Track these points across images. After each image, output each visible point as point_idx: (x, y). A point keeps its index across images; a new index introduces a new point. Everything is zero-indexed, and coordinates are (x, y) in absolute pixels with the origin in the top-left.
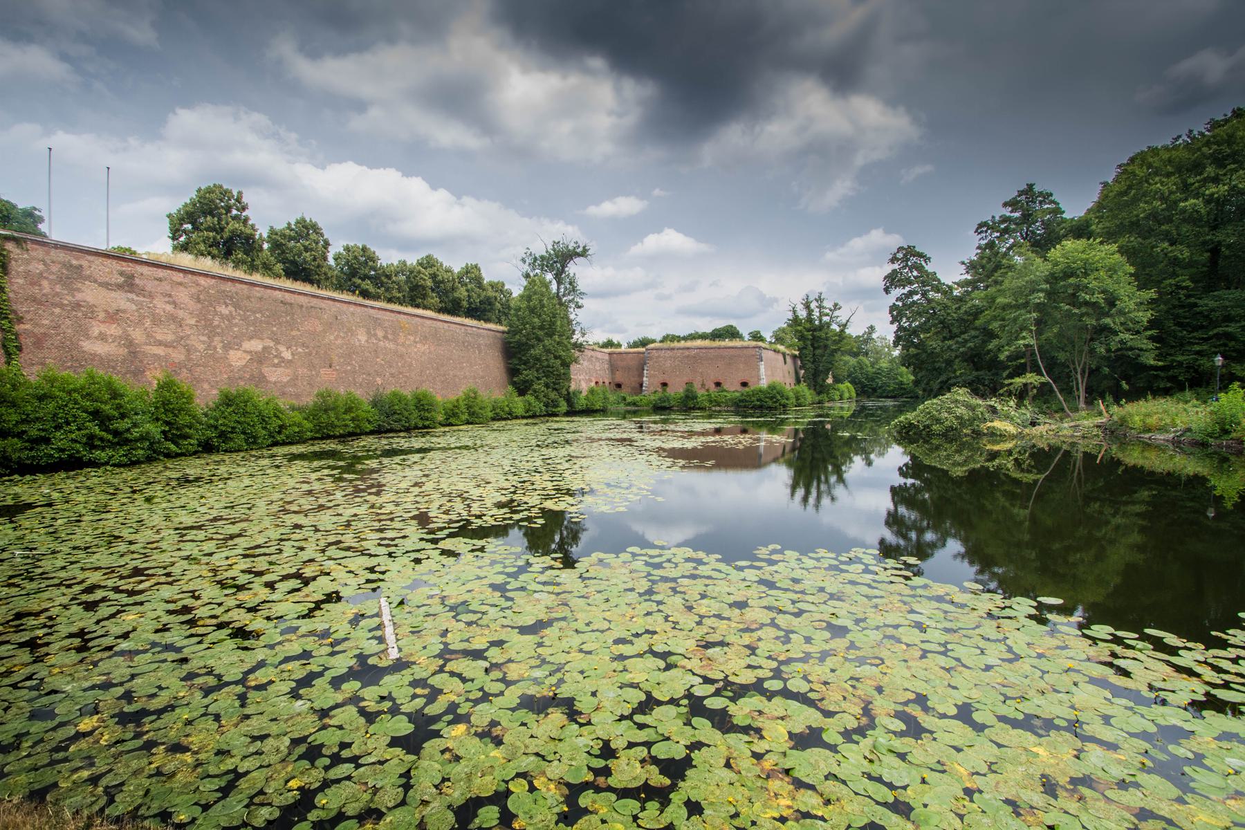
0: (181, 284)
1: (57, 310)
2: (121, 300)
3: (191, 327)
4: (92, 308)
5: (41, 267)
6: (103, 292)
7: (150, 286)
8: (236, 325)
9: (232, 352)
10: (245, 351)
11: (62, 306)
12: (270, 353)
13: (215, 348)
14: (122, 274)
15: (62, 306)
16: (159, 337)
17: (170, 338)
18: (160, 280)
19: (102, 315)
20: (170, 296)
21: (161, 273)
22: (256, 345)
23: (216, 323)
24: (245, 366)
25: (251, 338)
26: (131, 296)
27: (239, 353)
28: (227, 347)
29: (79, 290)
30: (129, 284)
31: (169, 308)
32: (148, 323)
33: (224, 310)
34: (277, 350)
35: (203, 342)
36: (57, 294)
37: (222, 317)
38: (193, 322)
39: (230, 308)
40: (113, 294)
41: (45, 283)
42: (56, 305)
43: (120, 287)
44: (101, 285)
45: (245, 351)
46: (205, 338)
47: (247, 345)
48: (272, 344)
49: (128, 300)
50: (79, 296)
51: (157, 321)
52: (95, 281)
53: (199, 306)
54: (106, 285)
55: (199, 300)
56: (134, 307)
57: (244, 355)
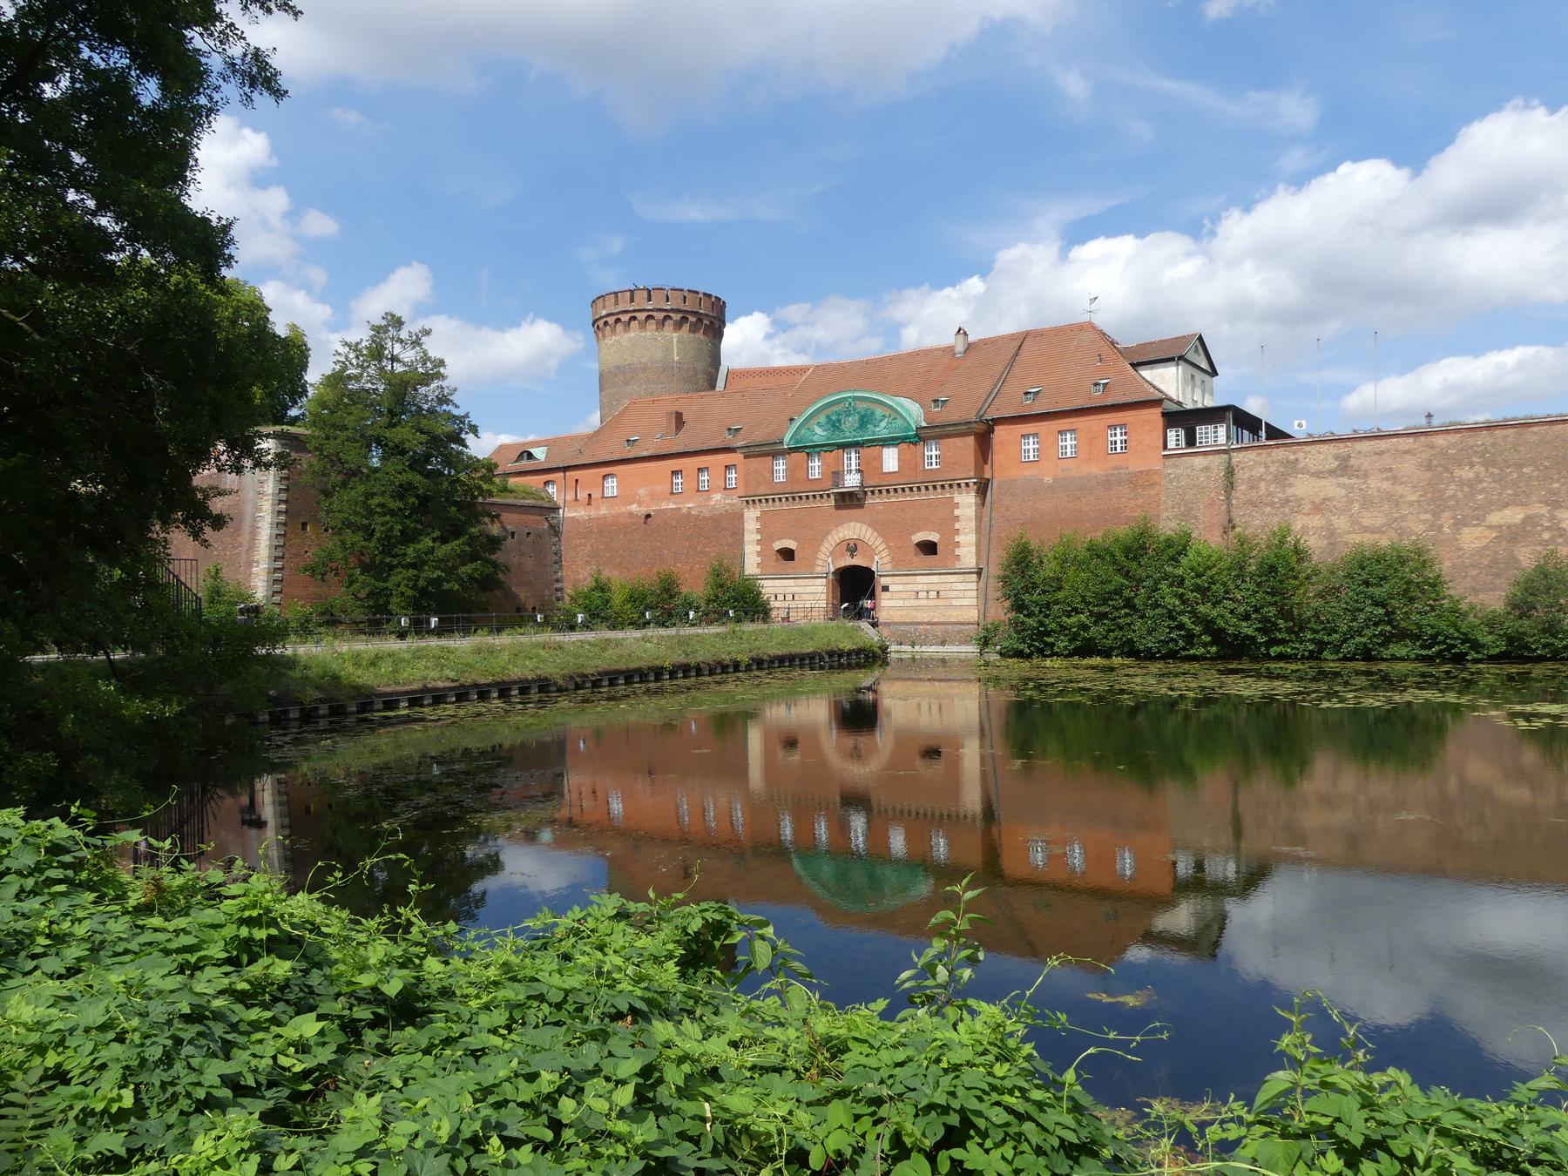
0: (1407, 452)
1: (1268, 509)
2: (1331, 488)
3: (1411, 504)
4: (1299, 501)
5: (1262, 470)
6: (1314, 482)
7: (1366, 464)
8: (1482, 491)
9: (1465, 531)
10: (1491, 527)
11: (1272, 504)
12: (1536, 524)
13: (1441, 527)
14: (1337, 457)
15: (1272, 504)
16: (1366, 522)
17: (1380, 521)
18: (1381, 453)
19: (1307, 507)
20: (1390, 470)
21: (1383, 444)
22: (1515, 515)
23: (1449, 493)
24: (1486, 547)
25: (1506, 505)
26: (1341, 480)
27: (1478, 531)
28: (1459, 525)
29: (1291, 485)
30: (1344, 468)
31: (1386, 485)
32: (1356, 507)
33: (1466, 473)
34: (1553, 517)
35: (1425, 522)
36: (1270, 494)
37: (1462, 483)
38: (1414, 497)
39: (1480, 469)
40: (1323, 482)
41: (1262, 485)
42: (1267, 505)
43: (1332, 472)
44: (1312, 475)
45: (1491, 527)
46: (1428, 516)
47: (1495, 518)
48: (1544, 510)
49: (1339, 485)
50: (1290, 491)
51: (1367, 503)
52: (1308, 472)
53: (1429, 474)
54: (1318, 475)
55: (1429, 467)
56: (1343, 492)
57: (1487, 532)
